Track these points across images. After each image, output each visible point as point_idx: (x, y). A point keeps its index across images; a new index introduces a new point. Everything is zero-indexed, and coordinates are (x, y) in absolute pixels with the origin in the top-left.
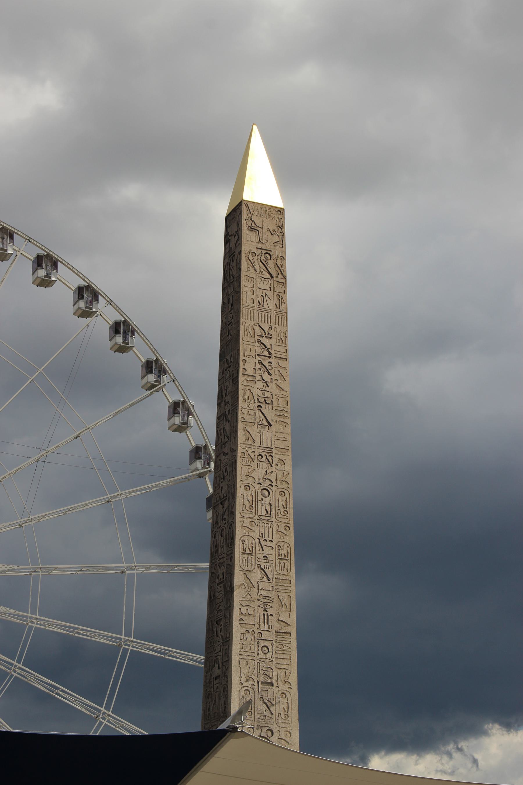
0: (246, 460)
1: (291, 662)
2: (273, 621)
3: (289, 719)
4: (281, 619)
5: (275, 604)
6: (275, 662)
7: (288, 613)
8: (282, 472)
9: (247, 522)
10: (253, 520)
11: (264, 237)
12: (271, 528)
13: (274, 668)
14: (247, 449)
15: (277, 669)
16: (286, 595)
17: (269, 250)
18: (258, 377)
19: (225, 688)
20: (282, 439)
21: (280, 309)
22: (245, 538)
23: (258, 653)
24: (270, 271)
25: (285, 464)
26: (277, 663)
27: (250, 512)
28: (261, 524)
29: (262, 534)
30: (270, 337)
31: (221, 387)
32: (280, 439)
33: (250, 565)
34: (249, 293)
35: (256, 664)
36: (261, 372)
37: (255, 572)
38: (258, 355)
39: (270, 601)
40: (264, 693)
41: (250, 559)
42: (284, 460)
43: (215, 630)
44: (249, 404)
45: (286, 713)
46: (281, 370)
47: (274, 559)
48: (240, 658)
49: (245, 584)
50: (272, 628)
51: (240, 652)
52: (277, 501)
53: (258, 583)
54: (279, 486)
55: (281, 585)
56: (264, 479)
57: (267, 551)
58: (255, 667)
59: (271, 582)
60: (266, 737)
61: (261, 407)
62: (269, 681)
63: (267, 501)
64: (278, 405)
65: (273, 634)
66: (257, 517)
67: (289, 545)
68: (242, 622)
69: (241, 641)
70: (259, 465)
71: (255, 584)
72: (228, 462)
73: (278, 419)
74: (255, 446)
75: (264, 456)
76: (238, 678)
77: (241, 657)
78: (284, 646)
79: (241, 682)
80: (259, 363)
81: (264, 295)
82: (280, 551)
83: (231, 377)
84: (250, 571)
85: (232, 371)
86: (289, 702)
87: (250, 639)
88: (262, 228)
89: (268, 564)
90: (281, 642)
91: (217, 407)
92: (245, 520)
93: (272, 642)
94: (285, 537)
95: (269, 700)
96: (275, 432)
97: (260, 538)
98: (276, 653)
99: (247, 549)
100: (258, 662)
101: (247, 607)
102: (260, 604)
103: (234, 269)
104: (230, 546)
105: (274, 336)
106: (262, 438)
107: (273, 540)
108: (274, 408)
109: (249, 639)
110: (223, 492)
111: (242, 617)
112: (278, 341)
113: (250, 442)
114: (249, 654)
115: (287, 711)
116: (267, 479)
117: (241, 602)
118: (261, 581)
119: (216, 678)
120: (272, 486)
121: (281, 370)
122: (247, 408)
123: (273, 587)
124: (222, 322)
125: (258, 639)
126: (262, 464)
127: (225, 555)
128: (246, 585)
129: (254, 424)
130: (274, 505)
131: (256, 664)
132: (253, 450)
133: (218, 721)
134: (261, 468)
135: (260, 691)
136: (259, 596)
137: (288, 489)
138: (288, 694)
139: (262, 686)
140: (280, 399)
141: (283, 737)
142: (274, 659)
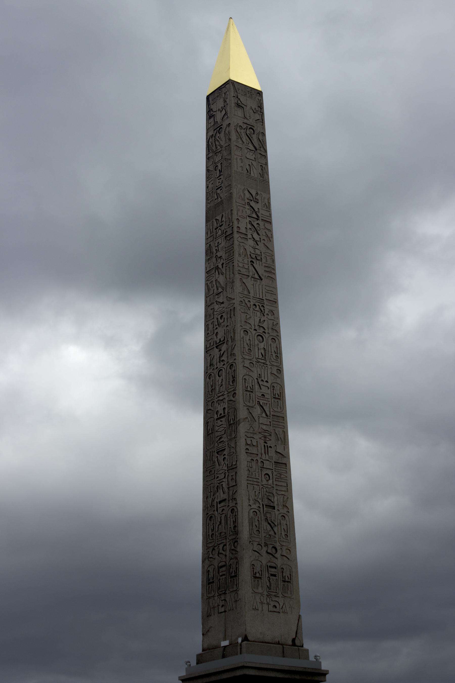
0: (244, 308)
1: (287, 489)
2: (272, 452)
3: (288, 538)
4: (278, 451)
5: (273, 438)
6: (275, 488)
7: (283, 446)
8: (272, 321)
9: (247, 364)
10: (252, 362)
11: (248, 114)
12: (266, 370)
13: (274, 493)
14: (244, 298)
15: (277, 495)
16: (281, 430)
17: (252, 126)
18: (249, 236)
19: (233, 510)
20: (271, 293)
21: (263, 178)
22: (246, 377)
23: (262, 480)
24: (254, 144)
25: (274, 315)
26: (277, 490)
27: (249, 355)
28: (258, 366)
29: (259, 374)
30: (257, 201)
32: (269, 292)
33: (251, 401)
34: (239, 161)
35: (261, 489)
36: (251, 232)
37: (256, 408)
38: (248, 216)
39: (269, 435)
40: (268, 515)
41: (251, 396)
42: (273, 311)
43: (216, 459)
44: (244, 258)
45: (286, 533)
46: (267, 231)
47: (270, 398)
48: (248, 483)
49: (248, 418)
50: (272, 458)
51: (248, 478)
52: (270, 346)
53: (259, 418)
54: (271, 334)
55: (276, 421)
56: (259, 327)
57: (264, 390)
58: (260, 491)
59: (269, 417)
60: (272, 553)
61: (253, 263)
62: (272, 505)
63: (262, 345)
64: (266, 263)
65: (272, 463)
66: (254, 360)
67: (281, 386)
68: (247, 451)
69: (248, 468)
70: (254, 313)
71: (256, 418)
72: (223, 310)
73: (267, 274)
74: (250, 296)
75: (258, 306)
76: (248, 501)
77: (249, 482)
78: (282, 475)
79: (250, 504)
80: (249, 223)
81: (250, 164)
82: (274, 391)
83: (224, 235)
84: (252, 407)
85: (225, 229)
86: (288, 524)
87: (255, 467)
88: (246, 106)
89: (266, 402)
90: (279, 471)
91: (205, 263)
92: (245, 361)
93: (272, 470)
94: (278, 379)
95: (273, 521)
96: (265, 285)
97: (258, 378)
98: (275, 480)
99: (249, 387)
100: (262, 488)
101: (251, 439)
102: (261, 436)
103: (221, 140)
105: (260, 201)
106: (255, 290)
107: (268, 381)
108: (264, 265)
109: (254, 467)
110: (219, 337)
111: (248, 447)
112: (263, 206)
113: (246, 292)
114: (255, 480)
115: (286, 532)
116: (261, 326)
117: (246, 433)
118: (261, 416)
119: (220, 502)
120: (265, 333)
121: (267, 231)
122: (242, 262)
123: (270, 422)
124: (207, 187)
125: (261, 467)
126: (256, 313)
127: (226, 393)
128: (249, 419)
129: (248, 277)
130: (268, 350)
131: (261, 489)
132: (249, 300)
133: (226, 539)
134: (256, 316)
135: (265, 513)
136: (260, 429)
137: (278, 337)
138: (286, 517)
139: (266, 509)
140: (267, 257)
141: (285, 554)
142: (274, 486)
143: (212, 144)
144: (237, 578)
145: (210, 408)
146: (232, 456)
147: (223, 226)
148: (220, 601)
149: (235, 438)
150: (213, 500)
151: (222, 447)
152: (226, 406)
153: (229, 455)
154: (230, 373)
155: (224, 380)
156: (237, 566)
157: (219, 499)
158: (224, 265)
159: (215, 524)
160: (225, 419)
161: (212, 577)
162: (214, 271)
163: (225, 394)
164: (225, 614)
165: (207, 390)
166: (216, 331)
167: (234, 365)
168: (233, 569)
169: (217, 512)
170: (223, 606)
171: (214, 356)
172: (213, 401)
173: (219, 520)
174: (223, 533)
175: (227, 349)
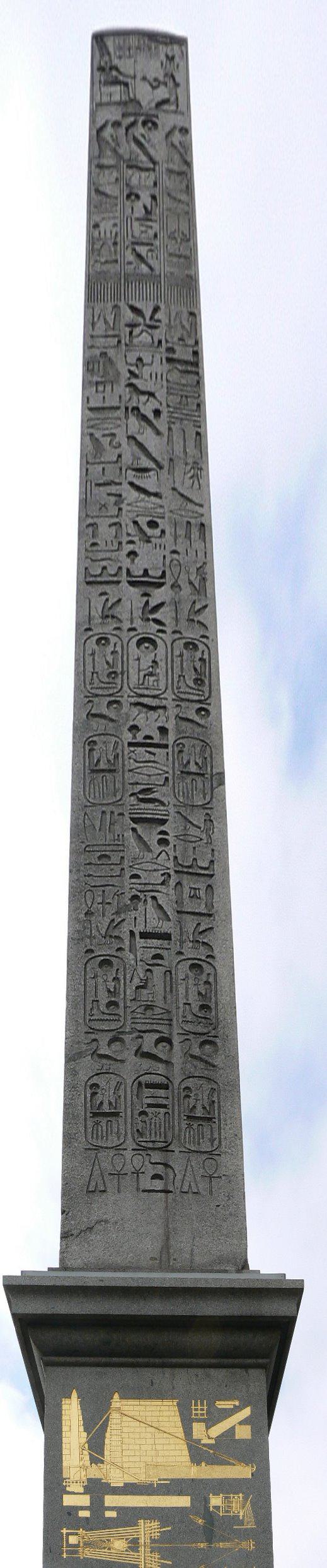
31: (104, 354)
119: (144, 935)
124: (93, 226)
127: (169, 695)
144: (215, 1126)
146: (194, 845)
147: (158, 331)
148: (147, 1163)
149: (203, 807)
150: (114, 925)
151: (155, 812)
152: (170, 726)
153: (183, 838)
154: (185, 657)
155: (162, 664)
156: (215, 1099)
157: (143, 926)
158: (164, 415)
160: (167, 753)
161: (110, 1103)
162: (120, 413)
163: (166, 699)
164: (167, 1198)
165: (89, 668)
167: (201, 647)
169: (132, 956)
170: (156, 1177)
171: (119, 600)
172: (118, 699)
173: (142, 976)
174: (159, 1009)
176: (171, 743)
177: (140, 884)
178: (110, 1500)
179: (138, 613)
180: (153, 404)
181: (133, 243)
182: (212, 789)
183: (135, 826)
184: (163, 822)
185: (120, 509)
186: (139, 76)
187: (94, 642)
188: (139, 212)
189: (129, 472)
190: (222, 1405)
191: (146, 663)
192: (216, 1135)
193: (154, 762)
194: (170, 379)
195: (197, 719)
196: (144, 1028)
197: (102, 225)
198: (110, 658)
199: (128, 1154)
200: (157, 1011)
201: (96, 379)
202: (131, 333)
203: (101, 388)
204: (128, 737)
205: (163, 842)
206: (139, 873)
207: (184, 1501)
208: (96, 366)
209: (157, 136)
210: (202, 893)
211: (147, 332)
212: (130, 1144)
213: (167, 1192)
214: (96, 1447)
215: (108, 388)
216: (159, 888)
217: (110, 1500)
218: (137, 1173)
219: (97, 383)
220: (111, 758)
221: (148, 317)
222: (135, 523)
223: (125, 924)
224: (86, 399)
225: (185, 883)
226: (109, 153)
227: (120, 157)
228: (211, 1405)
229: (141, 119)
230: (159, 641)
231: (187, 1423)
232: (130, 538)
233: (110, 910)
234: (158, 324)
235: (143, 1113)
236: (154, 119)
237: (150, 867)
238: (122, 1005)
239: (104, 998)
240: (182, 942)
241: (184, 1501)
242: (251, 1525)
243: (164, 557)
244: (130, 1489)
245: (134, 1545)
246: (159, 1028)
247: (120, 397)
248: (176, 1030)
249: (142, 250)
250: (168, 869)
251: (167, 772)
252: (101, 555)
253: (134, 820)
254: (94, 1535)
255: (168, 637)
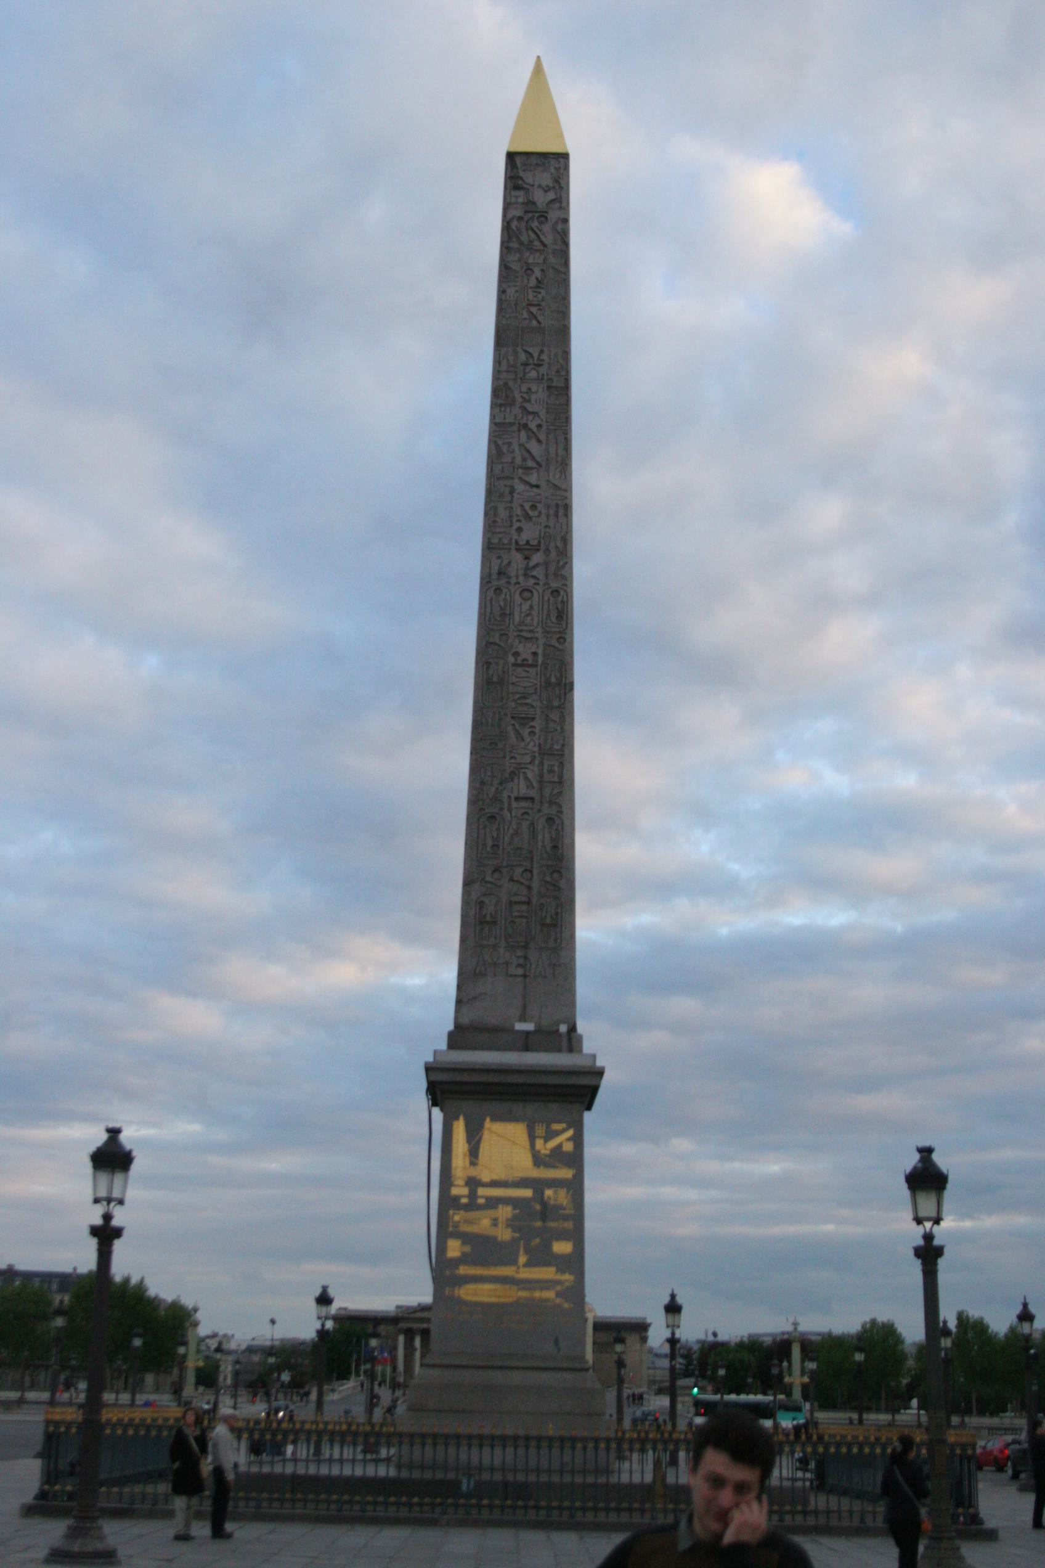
31: (506, 384)
104: (554, 619)
119: (517, 799)
124: (501, 291)
127: (540, 630)
143: (518, 230)
145: (497, 641)
149: (559, 707)
154: (551, 602)
155: (536, 608)
156: (559, 911)
158: (544, 427)
159: (504, 831)
160: (537, 671)
161: (491, 914)
162: (515, 428)
163: (538, 632)
165: (488, 610)
166: (516, 525)
167: (562, 593)
168: (547, 911)
169: (509, 814)
170: (519, 966)
172: (507, 632)
173: (515, 827)
175: (546, 564)
176: (540, 663)
177: (516, 763)
178: (481, 1191)
179: (521, 572)
180: (537, 421)
181: (528, 305)
182: (565, 694)
183: (513, 722)
184: (533, 719)
185: (513, 497)
186: (537, 184)
187: (492, 591)
188: (533, 282)
189: (520, 470)
190: (556, 1127)
191: (526, 607)
192: (559, 935)
193: (528, 677)
194: (549, 402)
195: (557, 645)
196: (515, 863)
197: (508, 291)
198: (502, 604)
199: (502, 951)
200: (525, 852)
201: (499, 401)
202: (524, 369)
203: (503, 409)
204: (511, 659)
205: (532, 733)
206: (516, 756)
207: (527, 1193)
208: (500, 393)
209: (547, 228)
210: (556, 769)
211: (535, 369)
212: (503, 943)
213: (525, 976)
214: (474, 1153)
215: (508, 410)
216: (528, 766)
217: (481, 1191)
218: (507, 963)
219: (501, 405)
220: (500, 673)
221: (536, 358)
222: (522, 506)
223: (505, 791)
224: (493, 417)
225: (545, 761)
226: (514, 240)
227: (521, 243)
228: (548, 1127)
229: (537, 215)
230: (534, 591)
231: (532, 1138)
232: (518, 518)
233: (496, 782)
234: (542, 363)
235: (512, 922)
236: (545, 214)
237: (523, 752)
238: (501, 848)
239: (490, 843)
240: (541, 803)
241: (527, 1193)
242: (570, 1212)
243: (540, 530)
244: (494, 1184)
245: (495, 1222)
246: (525, 863)
247: (515, 416)
248: (535, 865)
249: (534, 310)
250: (534, 752)
251: (536, 684)
252: (498, 530)
253: (513, 718)
254: (472, 1215)
255: (540, 588)
